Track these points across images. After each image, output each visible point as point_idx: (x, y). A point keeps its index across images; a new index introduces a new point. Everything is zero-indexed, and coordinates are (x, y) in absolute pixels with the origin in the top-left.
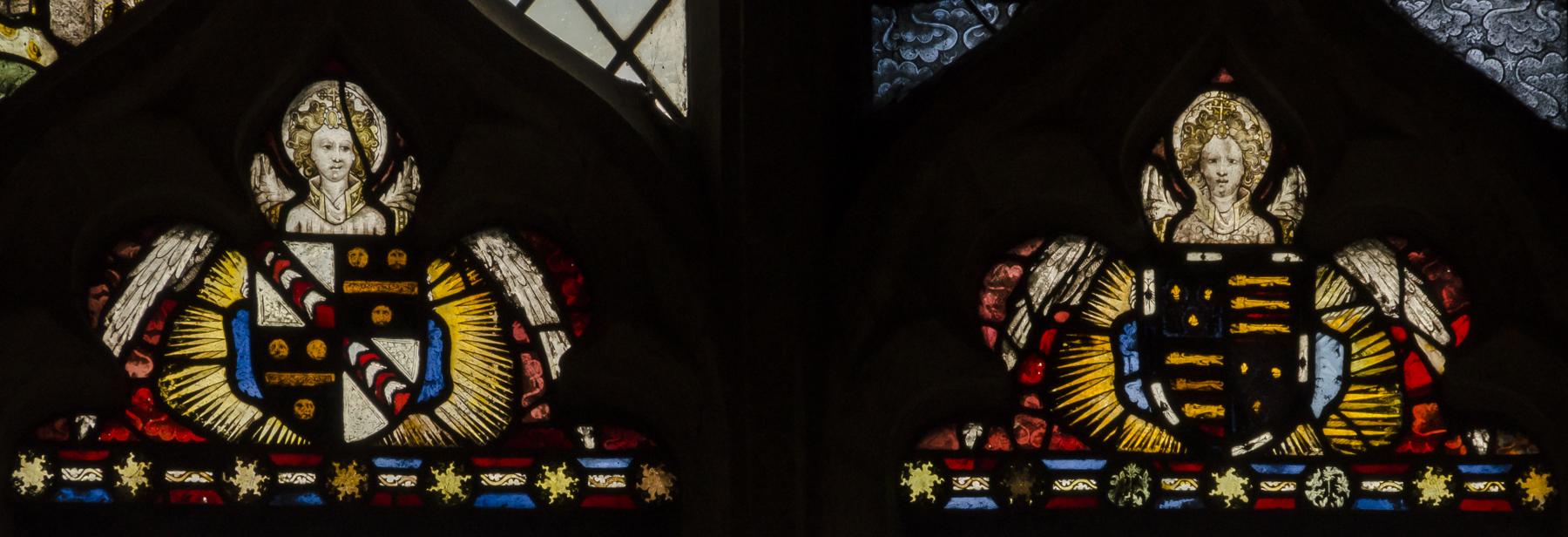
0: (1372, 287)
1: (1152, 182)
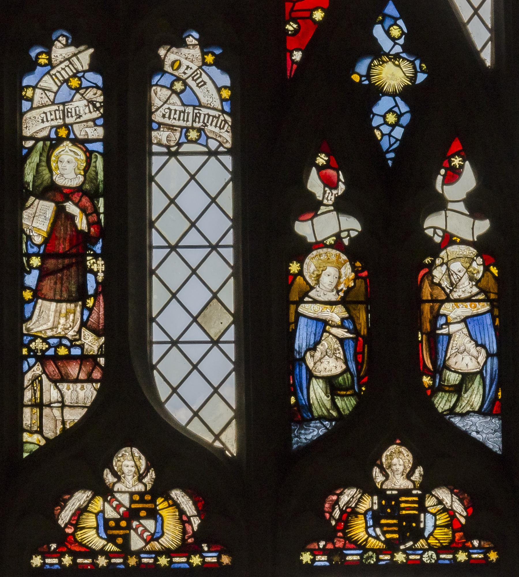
1: (376, 471)
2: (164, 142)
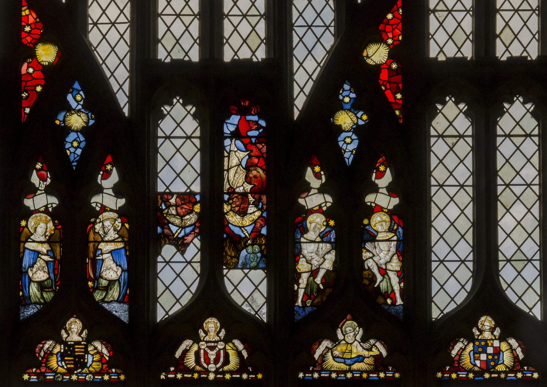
0: (97, 347)
1: (63, 332)
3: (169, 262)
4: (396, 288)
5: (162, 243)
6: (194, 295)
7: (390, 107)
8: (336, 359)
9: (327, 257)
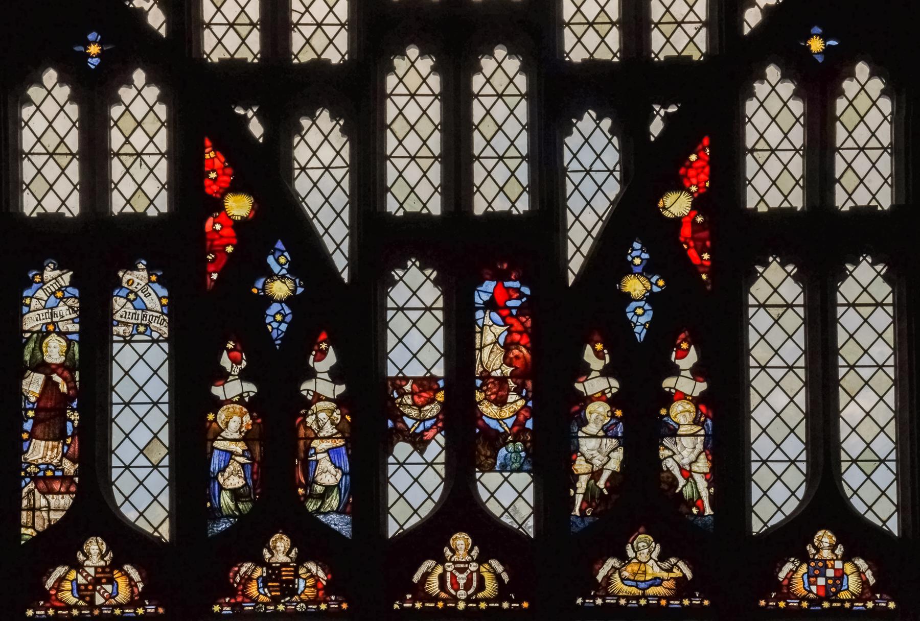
0: (311, 570)
1: (265, 551)
2: (122, 333)
3: (404, 463)
4: (705, 494)
5: (393, 439)
6: (437, 504)
7: (695, 272)
8: (625, 582)
9: (613, 455)
